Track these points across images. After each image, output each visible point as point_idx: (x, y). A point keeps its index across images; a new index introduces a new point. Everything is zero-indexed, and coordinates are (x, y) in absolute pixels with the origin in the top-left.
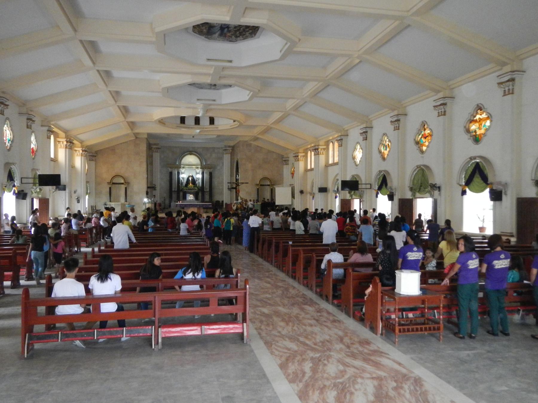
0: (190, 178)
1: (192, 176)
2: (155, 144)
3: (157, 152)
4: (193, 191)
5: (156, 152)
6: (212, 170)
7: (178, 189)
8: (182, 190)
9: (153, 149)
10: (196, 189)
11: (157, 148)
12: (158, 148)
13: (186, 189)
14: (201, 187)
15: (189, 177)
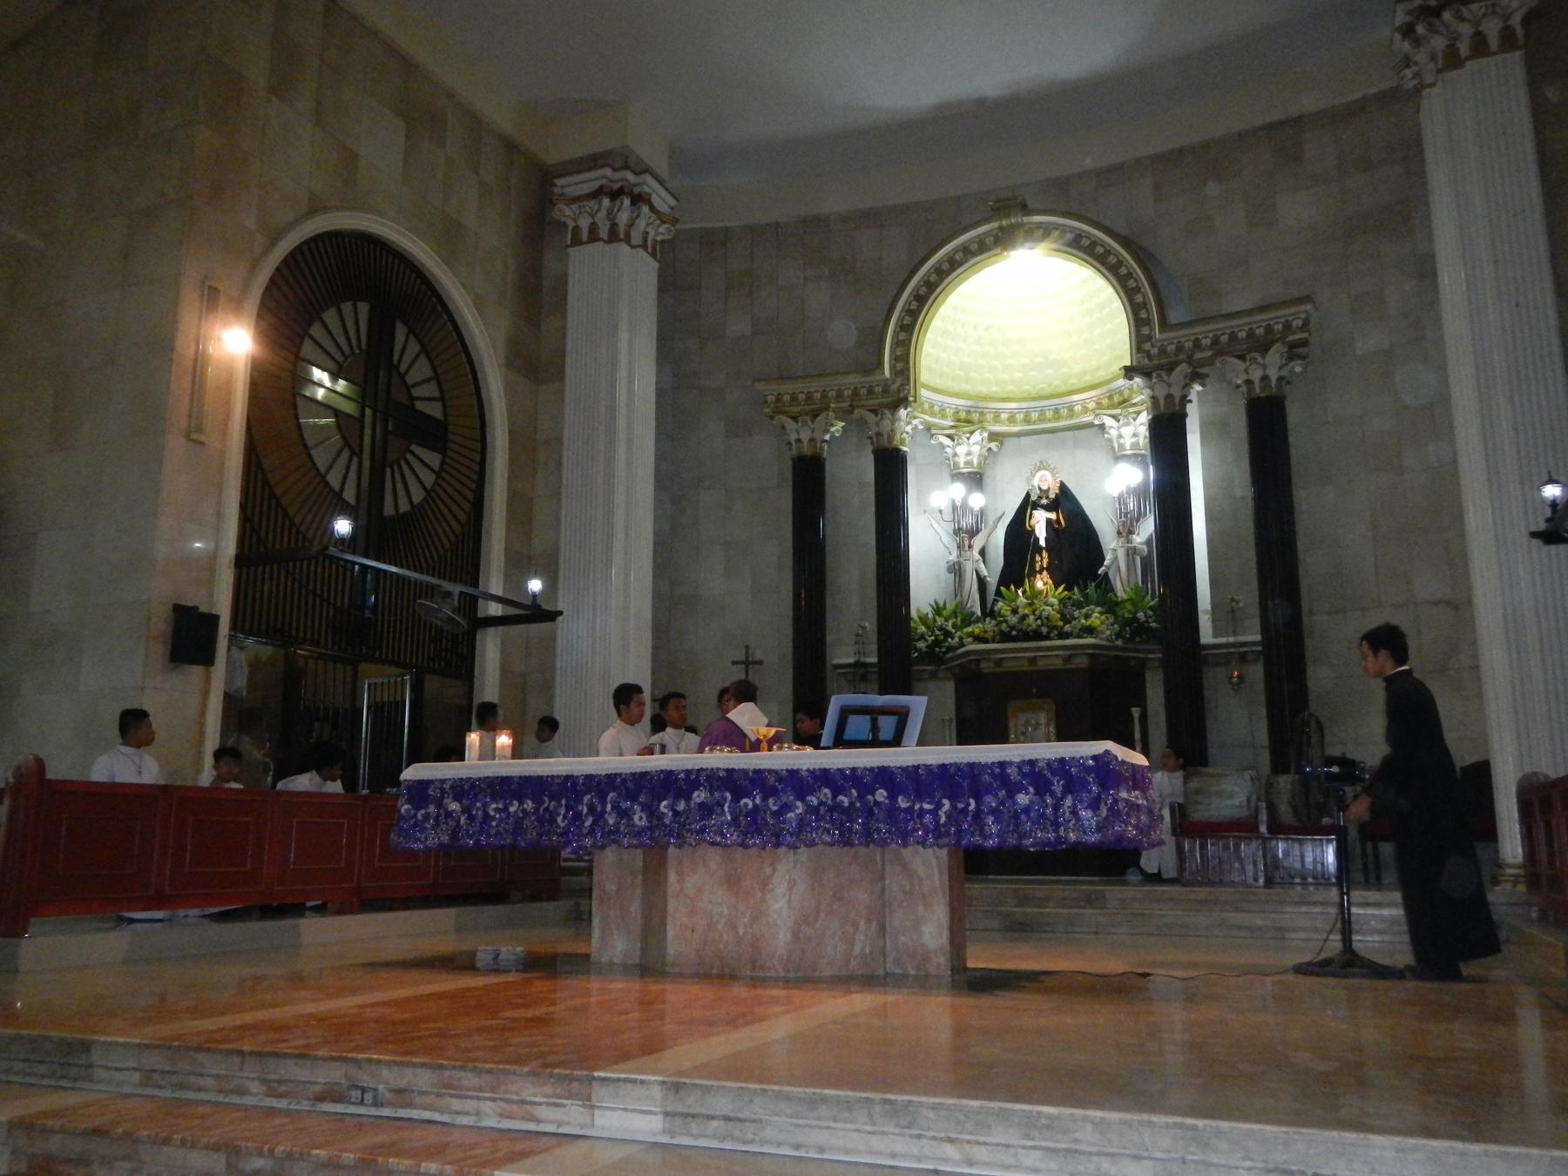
0: (1040, 521)
1: (1063, 501)
2: (594, 161)
3: (613, 237)
4: (1051, 653)
5: (594, 236)
6: (1273, 363)
7: (882, 652)
8: (937, 655)
9: (565, 213)
10: (1090, 631)
11: (596, 194)
12: (615, 195)
13: (978, 639)
14: (1160, 610)
15: (1028, 505)
